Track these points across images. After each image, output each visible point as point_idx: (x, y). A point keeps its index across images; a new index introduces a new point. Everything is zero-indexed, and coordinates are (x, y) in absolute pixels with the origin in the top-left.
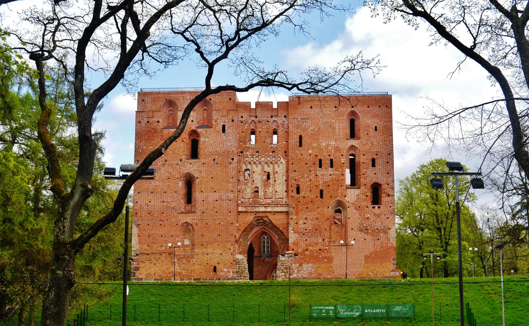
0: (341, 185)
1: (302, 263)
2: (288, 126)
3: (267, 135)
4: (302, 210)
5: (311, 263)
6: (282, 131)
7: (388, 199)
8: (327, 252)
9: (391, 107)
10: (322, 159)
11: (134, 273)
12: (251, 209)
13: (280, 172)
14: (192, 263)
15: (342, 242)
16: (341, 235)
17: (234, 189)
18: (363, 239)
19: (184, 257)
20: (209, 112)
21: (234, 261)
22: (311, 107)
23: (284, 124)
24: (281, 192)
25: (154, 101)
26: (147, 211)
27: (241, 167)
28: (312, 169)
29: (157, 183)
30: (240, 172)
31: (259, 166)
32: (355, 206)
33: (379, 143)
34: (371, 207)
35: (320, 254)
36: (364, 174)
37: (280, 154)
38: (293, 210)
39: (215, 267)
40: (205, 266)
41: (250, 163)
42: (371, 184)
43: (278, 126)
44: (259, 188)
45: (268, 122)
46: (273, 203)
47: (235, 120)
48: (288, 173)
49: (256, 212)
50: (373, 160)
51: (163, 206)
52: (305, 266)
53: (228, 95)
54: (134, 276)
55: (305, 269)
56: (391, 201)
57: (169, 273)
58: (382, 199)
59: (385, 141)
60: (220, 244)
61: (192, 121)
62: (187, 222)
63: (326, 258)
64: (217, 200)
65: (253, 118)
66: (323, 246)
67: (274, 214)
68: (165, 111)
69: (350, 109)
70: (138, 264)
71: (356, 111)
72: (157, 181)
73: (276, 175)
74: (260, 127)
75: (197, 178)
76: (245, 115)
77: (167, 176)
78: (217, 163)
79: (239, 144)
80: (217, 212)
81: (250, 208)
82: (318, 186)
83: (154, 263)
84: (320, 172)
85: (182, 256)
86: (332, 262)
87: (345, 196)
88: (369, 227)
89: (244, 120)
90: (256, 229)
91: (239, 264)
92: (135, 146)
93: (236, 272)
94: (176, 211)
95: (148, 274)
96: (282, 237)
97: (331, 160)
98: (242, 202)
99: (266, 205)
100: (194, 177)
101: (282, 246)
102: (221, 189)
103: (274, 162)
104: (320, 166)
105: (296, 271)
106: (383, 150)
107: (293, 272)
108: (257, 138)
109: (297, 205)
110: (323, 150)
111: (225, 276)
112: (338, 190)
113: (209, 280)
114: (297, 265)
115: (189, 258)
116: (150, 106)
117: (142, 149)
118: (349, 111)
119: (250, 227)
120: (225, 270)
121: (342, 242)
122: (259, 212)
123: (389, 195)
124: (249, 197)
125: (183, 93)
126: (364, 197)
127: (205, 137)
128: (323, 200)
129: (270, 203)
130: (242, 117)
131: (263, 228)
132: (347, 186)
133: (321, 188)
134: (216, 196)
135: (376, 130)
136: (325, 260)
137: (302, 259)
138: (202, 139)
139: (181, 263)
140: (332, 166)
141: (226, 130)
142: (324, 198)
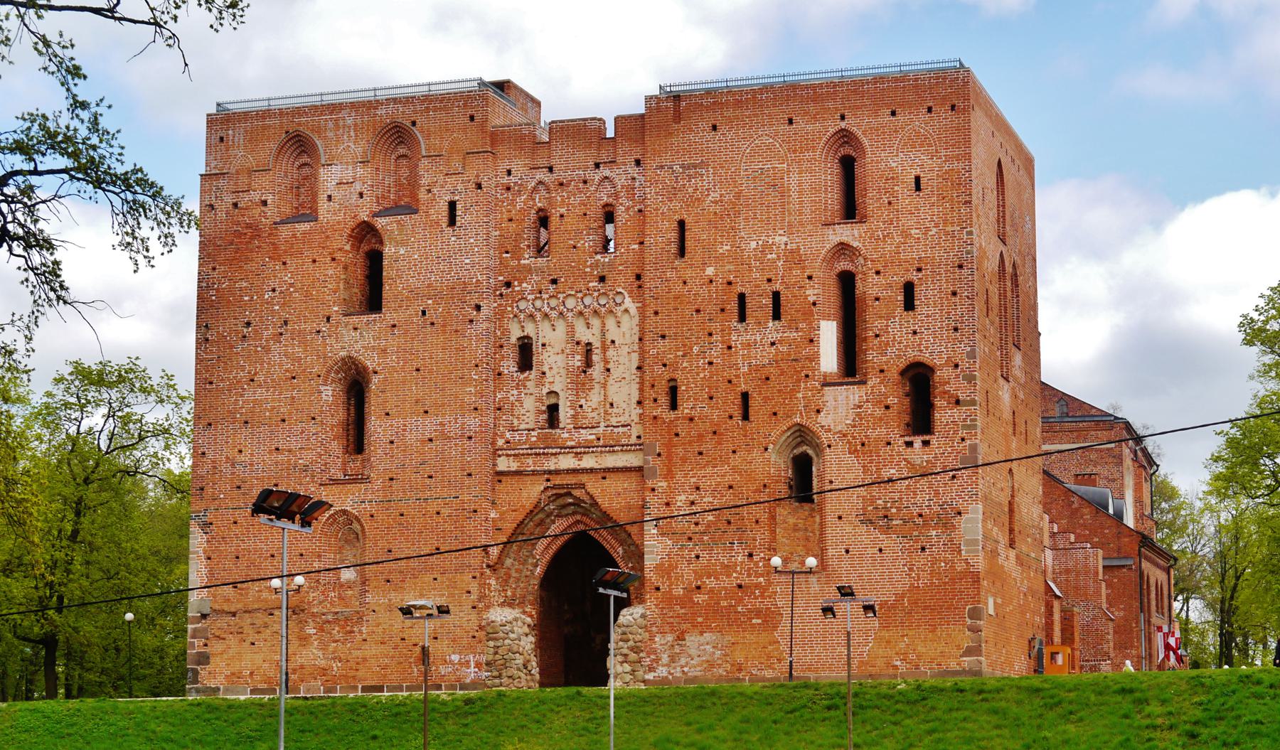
0: (807, 376)
1: (683, 632)
3: (582, 227)
4: (684, 460)
5: (711, 630)
6: (628, 209)
7: (957, 413)
8: (762, 596)
10: (747, 291)
11: (196, 672)
12: (535, 464)
13: (622, 341)
14: (359, 638)
15: (811, 562)
16: (807, 539)
17: (480, 403)
18: (876, 550)
19: (336, 621)
21: (481, 628)
22: (714, 128)
23: (633, 189)
24: (624, 405)
25: (253, 139)
26: (232, 480)
27: (506, 332)
28: (715, 327)
29: (261, 394)
31: (561, 326)
32: (849, 442)
33: (928, 229)
34: (901, 441)
36: (877, 336)
37: (621, 283)
40: (396, 648)
41: (532, 316)
42: (902, 366)
43: (616, 196)
44: (561, 394)
45: (585, 182)
47: (484, 185)
49: (550, 472)
50: (909, 289)
51: (276, 463)
52: (692, 640)
53: (465, 105)
54: (196, 682)
55: (693, 652)
56: (965, 420)
58: (937, 415)
60: (438, 577)
61: (361, 195)
62: (344, 512)
63: (758, 613)
64: (431, 440)
65: (542, 175)
66: (749, 575)
67: (604, 478)
68: (287, 170)
69: (833, 126)
70: (206, 645)
72: (260, 386)
74: (563, 201)
75: (376, 373)
76: (519, 167)
77: (287, 371)
78: (432, 324)
79: (501, 258)
80: (430, 477)
81: (530, 461)
82: (735, 381)
83: (251, 639)
84: (740, 336)
85: (330, 617)
86: (775, 628)
87: (818, 411)
88: (894, 510)
92: (200, 281)
93: (488, 664)
94: (313, 476)
95: (233, 674)
97: (776, 296)
98: (508, 442)
99: (580, 450)
100: (365, 368)
102: (443, 405)
103: (603, 310)
104: (742, 318)
105: (665, 658)
106: (938, 254)
107: (657, 660)
109: (669, 446)
111: (453, 678)
112: (794, 391)
114: (670, 638)
115: (349, 622)
116: (241, 156)
117: (217, 290)
118: (832, 130)
120: (455, 658)
121: (811, 562)
122: (557, 472)
123: (958, 402)
125: (334, 108)
126: (879, 412)
127: (397, 244)
129: (592, 441)
131: (578, 522)
132: (825, 376)
133: (743, 387)
134: (429, 426)
135: (918, 188)
136: (754, 621)
138: (388, 250)
139: (326, 637)
140: (777, 316)
141: (458, 218)
142: (752, 418)
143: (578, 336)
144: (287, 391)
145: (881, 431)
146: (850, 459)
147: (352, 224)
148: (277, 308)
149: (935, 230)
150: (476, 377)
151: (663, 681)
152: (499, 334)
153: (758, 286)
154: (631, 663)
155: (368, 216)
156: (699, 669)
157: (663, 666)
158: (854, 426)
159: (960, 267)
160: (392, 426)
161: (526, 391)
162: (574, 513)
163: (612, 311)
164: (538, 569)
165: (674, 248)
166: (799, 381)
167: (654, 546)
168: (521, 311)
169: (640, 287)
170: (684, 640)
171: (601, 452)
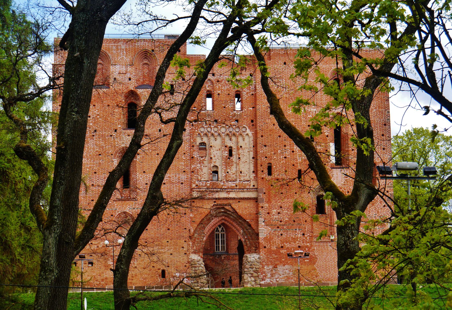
1: (276, 265)
2: (255, 87)
3: (228, 99)
4: (275, 196)
5: (288, 264)
6: (247, 93)
13: (245, 146)
17: (187, 169)
20: (151, 67)
21: (189, 262)
22: (285, 63)
24: (247, 173)
27: (195, 140)
30: (193, 146)
31: (219, 139)
37: (245, 123)
38: (264, 196)
39: (163, 272)
40: (150, 270)
41: (206, 135)
44: (219, 167)
46: (238, 187)
48: (256, 149)
49: (216, 199)
52: (280, 268)
55: (281, 273)
57: (103, 280)
59: (379, 107)
61: (130, 79)
62: (125, 213)
66: (303, 242)
67: (239, 202)
73: (241, 151)
77: (97, 151)
82: (296, 165)
86: (314, 263)
90: (214, 221)
91: (195, 267)
96: (250, 230)
101: (248, 243)
103: (238, 133)
105: (269, 275)
107: (265, 276)
108: (215, 103)
113: (156, 288)
114: (271, 267)
119: (208, 218)
122: (219, 199)
124: (206, 179)
129: (234, 187)
131: (223, 219)
133: (299, 168)
136: (306, 261)
137: (277, 259)
143: (226, 144)
144: (97, 160)
147: (126, 91)
148: (91, 124)
149: (375, 110)
150: (184, 158)
151: (268, 285)
152: (192, 141)
153: (304, 128)
154: (254, 277)
155: (133, 88)
156: (283, 279)
157: (268, 278)
158: (345, 185)
160: (147, 177)
161: (204, 165)
162: (222, 216)
163: (241, 134)
164: (205, 238)
167: (263, 230)
168: (201, 132)
169: (253, 125)
170: (277, 268)
171: (238, 191)
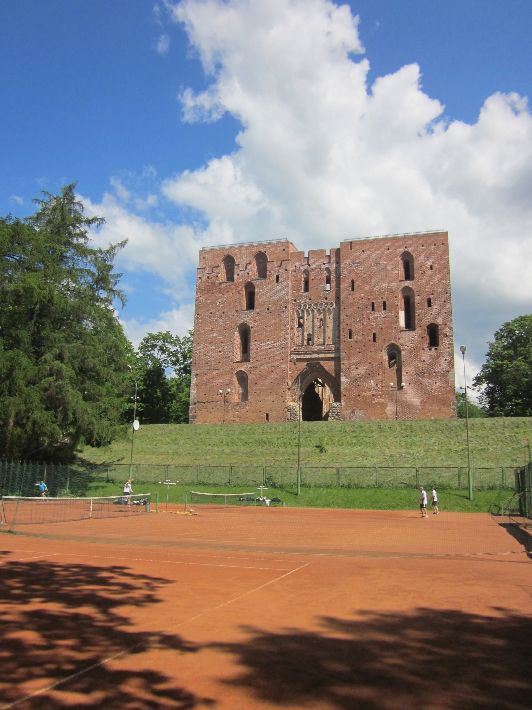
9: (447, 244)
11: (192, 421)
29: (215, 334)
32: (410, 348)
33: (435, 281)
35: (373, 399)
36: (419, 315)
63: (379, 403)
64: (270, 348)
66: (376, 391)
69: (403, 250)
71: (410, 251)
72: (215, 332)
77: (224, 327)
83: (210, 411)
84: (372, 315)
86: (385, 408)
87: (399, 339)
88: (425, 371)
89: (298, 270)
97: (384, 303)
100: (248, 327)
104: (373, 309)
110: (375, 293)
114: (349, 412)
118: (402, 251)
123: (447, 336)
126: (420, 339)
127: (260, 288)
128: (376, 344)
129: (323, 349)
130: (296, 266)
133: (374, 332)
134: (269, 344)
138: (257, 290)
145: (421, 345)
146: (410, 354)
159: (447, 293)
165: (350, 288)
166: (392, 329)
